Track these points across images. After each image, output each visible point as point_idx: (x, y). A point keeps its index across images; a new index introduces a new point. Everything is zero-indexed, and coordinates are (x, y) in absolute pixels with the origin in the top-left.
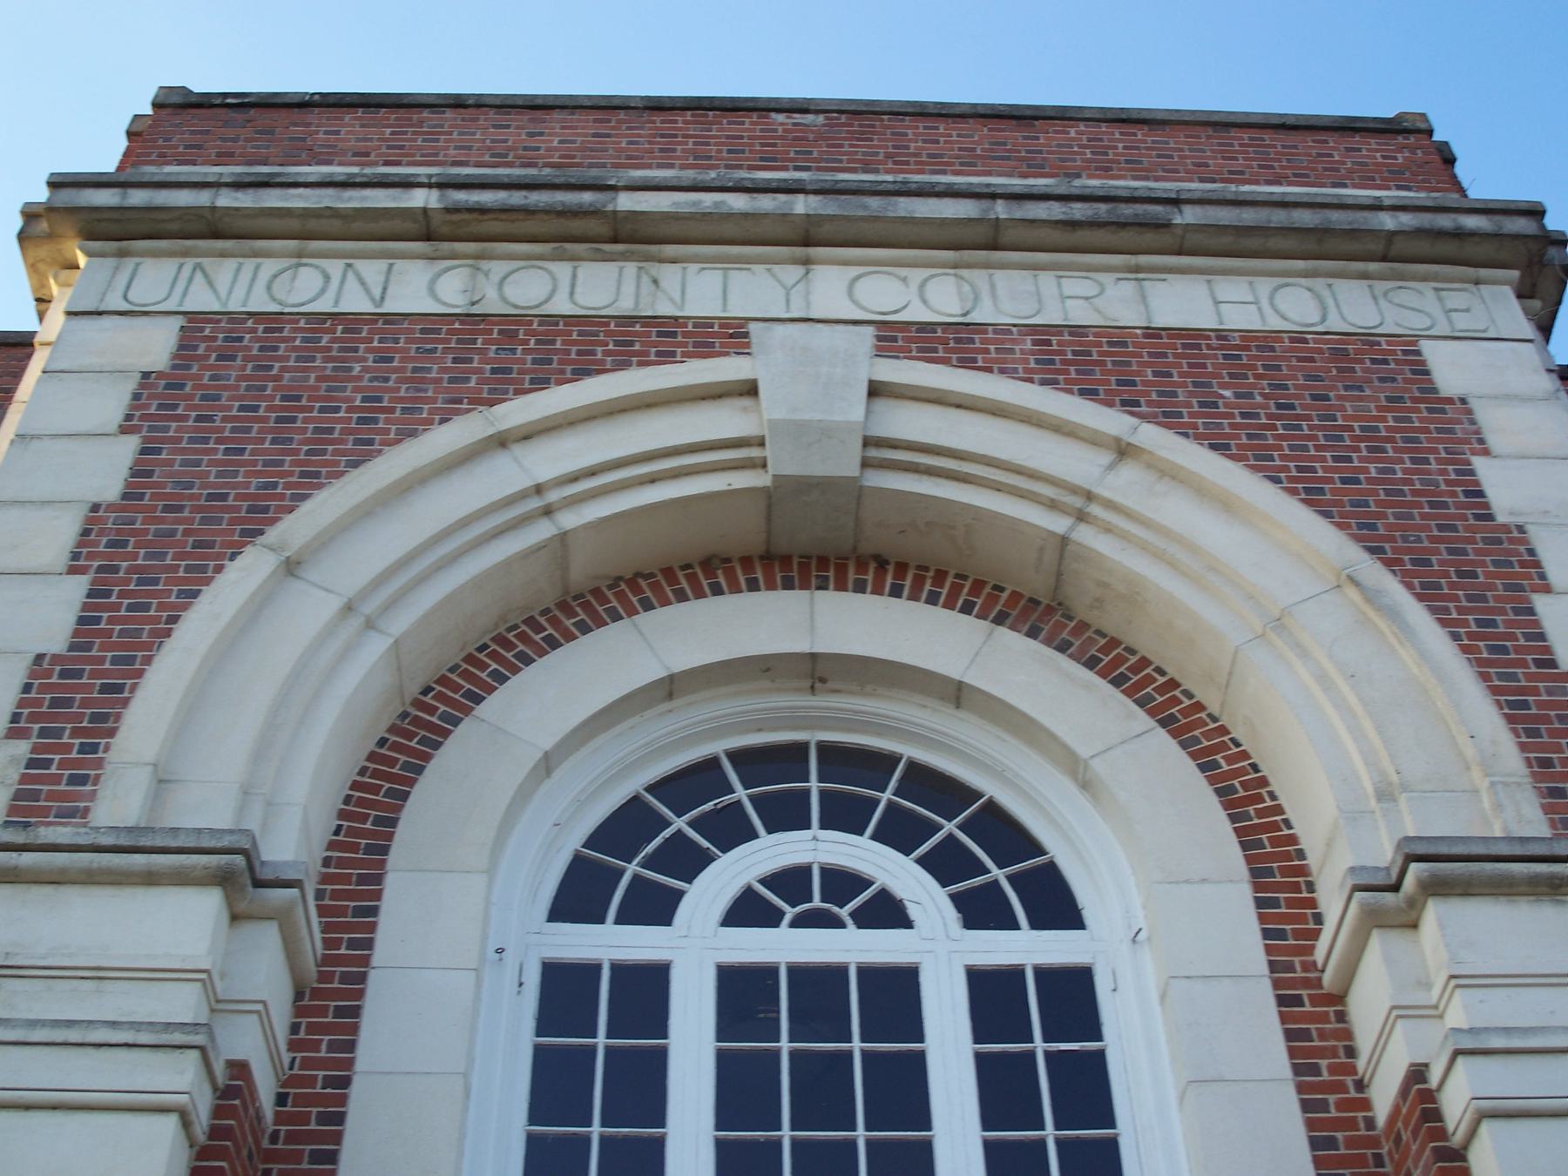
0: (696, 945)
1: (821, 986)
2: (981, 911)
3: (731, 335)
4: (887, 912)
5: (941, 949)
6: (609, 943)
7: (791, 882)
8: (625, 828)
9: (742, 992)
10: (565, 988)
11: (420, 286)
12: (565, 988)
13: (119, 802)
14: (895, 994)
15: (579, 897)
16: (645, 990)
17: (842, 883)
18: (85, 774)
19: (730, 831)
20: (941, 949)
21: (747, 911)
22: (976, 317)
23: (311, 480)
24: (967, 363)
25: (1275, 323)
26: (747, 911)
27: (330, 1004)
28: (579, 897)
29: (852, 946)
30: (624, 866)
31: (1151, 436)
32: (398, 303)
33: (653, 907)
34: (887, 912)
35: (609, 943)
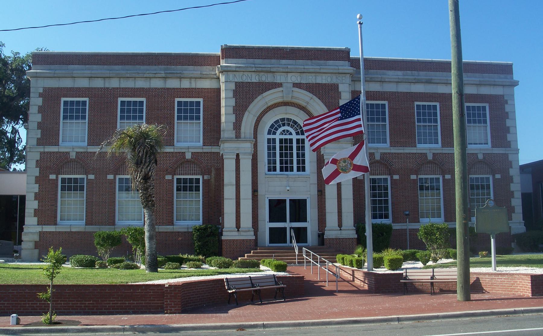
0: (278, 137)
1: (286, 140)
2: (297, 134)
3: (280, 85)
4: (291, 134)
5: (294, 137)
6: (272, 137)
7: (284, 131)
8: (272, 126)
9: (281, 141)
10: (269, 140)
11: (255, 78)
12: (269, 140)
13: (242, 135)
14: (291, 140)
15: (269, 133)
16: (274, 140)
17: (288, 131)
18: (240, 134)
19: (280, 126)
20: (294, 137)
21: (282, 134)
22: (302, 82)
23: (250, 104)
24: (300, 88)
25: (327, 82)
26: (282, 134)
27: (255, 146)
28: (269, 133)
29: (288, 137)
30: (273, 130)
31: (314, 97)
32: (254, 80)
33: (274, 133)
34: (291, 134)
35: (272, 137)
